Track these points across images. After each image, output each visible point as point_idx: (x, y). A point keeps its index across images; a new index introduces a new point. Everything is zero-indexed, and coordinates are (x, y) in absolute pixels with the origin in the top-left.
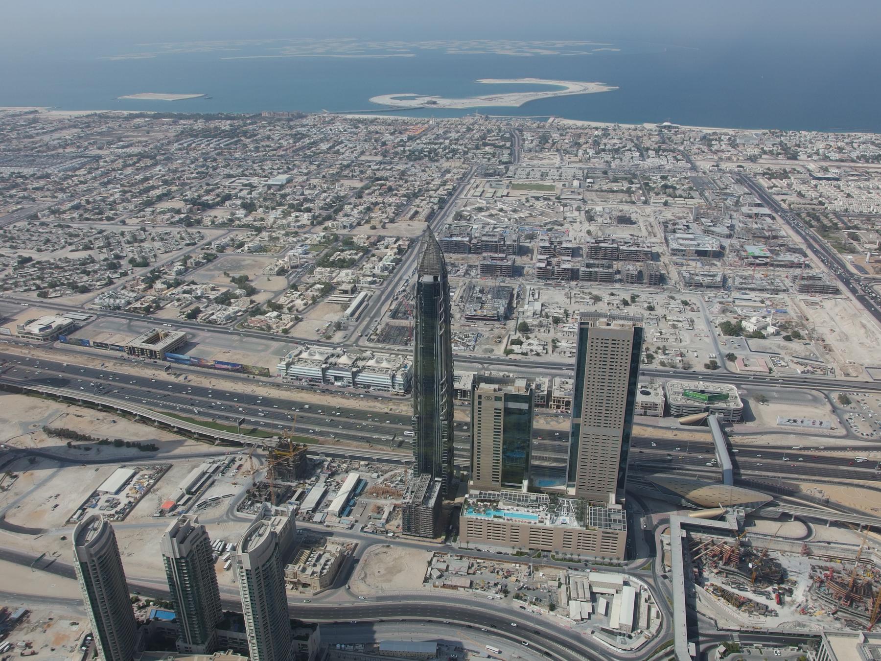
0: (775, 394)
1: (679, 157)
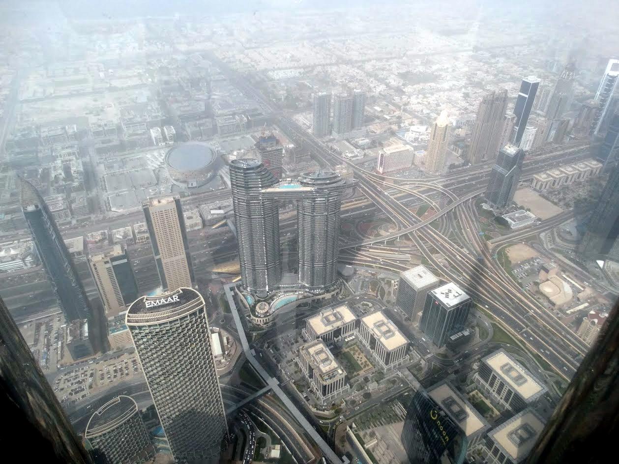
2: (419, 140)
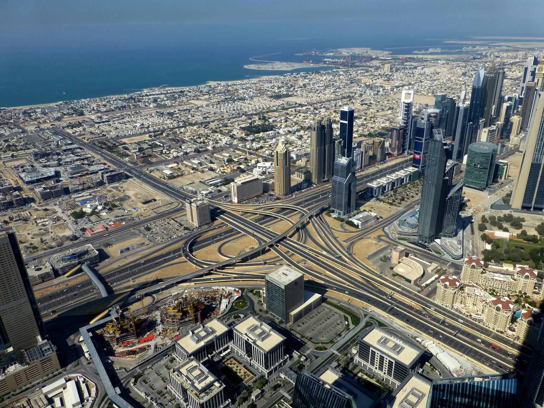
0: (114, 240)
1: (12, 127)
2: (267, 173)
